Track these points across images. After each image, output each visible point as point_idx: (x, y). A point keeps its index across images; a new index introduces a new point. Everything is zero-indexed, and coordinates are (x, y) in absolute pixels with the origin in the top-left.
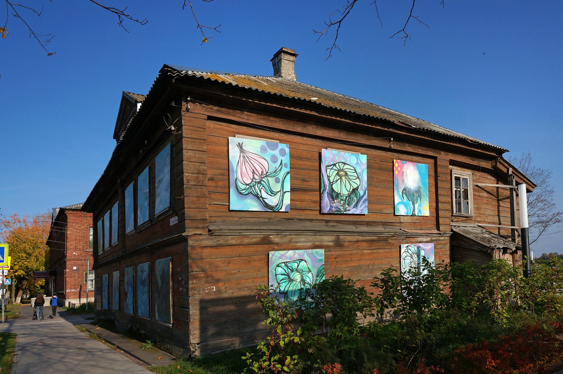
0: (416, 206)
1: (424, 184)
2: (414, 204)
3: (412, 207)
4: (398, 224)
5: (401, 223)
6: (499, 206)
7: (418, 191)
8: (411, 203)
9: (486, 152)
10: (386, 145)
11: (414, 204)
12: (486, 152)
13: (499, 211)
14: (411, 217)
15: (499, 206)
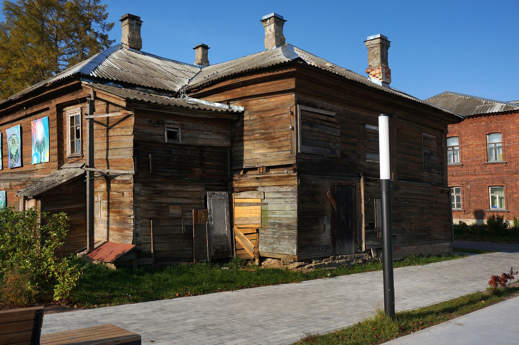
0: (42, 154)
1: (46, 134)
2: (41, 153)
3: (40, 155)
4: (36, 171)
5: (37, 170)
6: (108, 136)
7: (43, 142)
8: (39, 152)
9: (70, 84)
10: (23, 114)
11: (41, 153)
12: (70, 84)
13: (108, 142)
14: (40, 165)
15: (108, 136)
